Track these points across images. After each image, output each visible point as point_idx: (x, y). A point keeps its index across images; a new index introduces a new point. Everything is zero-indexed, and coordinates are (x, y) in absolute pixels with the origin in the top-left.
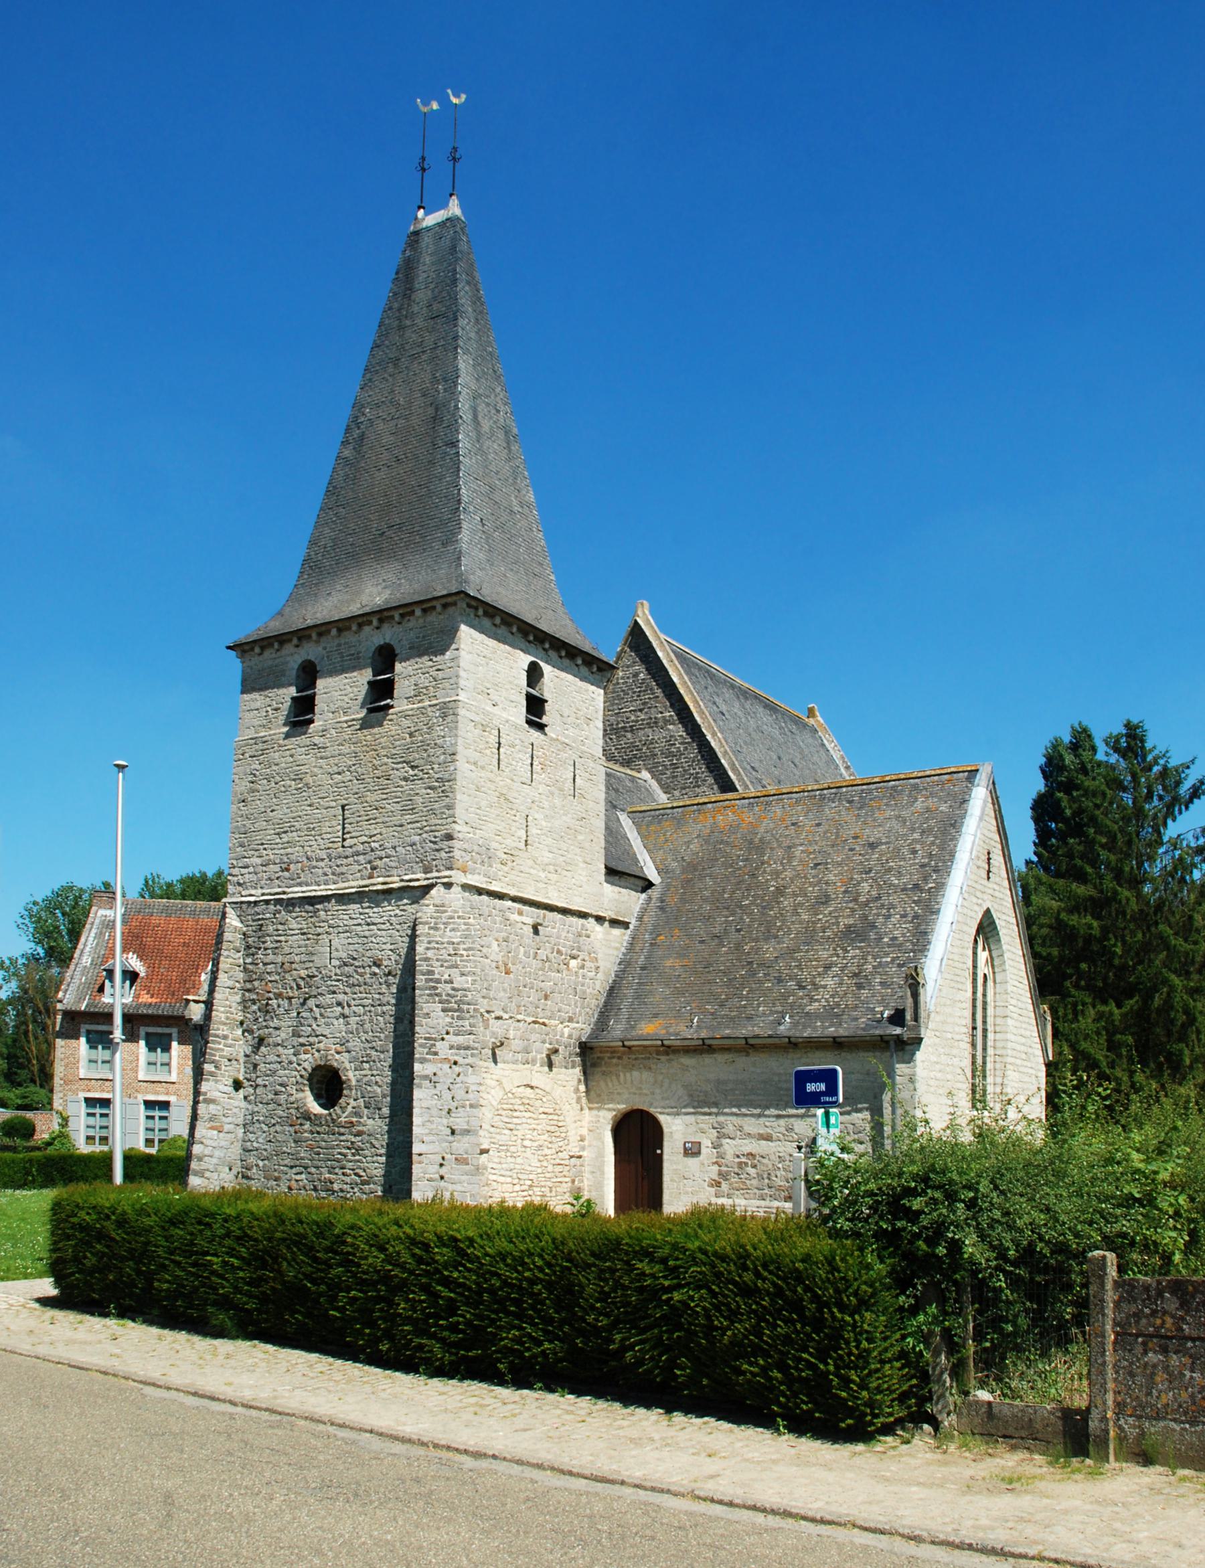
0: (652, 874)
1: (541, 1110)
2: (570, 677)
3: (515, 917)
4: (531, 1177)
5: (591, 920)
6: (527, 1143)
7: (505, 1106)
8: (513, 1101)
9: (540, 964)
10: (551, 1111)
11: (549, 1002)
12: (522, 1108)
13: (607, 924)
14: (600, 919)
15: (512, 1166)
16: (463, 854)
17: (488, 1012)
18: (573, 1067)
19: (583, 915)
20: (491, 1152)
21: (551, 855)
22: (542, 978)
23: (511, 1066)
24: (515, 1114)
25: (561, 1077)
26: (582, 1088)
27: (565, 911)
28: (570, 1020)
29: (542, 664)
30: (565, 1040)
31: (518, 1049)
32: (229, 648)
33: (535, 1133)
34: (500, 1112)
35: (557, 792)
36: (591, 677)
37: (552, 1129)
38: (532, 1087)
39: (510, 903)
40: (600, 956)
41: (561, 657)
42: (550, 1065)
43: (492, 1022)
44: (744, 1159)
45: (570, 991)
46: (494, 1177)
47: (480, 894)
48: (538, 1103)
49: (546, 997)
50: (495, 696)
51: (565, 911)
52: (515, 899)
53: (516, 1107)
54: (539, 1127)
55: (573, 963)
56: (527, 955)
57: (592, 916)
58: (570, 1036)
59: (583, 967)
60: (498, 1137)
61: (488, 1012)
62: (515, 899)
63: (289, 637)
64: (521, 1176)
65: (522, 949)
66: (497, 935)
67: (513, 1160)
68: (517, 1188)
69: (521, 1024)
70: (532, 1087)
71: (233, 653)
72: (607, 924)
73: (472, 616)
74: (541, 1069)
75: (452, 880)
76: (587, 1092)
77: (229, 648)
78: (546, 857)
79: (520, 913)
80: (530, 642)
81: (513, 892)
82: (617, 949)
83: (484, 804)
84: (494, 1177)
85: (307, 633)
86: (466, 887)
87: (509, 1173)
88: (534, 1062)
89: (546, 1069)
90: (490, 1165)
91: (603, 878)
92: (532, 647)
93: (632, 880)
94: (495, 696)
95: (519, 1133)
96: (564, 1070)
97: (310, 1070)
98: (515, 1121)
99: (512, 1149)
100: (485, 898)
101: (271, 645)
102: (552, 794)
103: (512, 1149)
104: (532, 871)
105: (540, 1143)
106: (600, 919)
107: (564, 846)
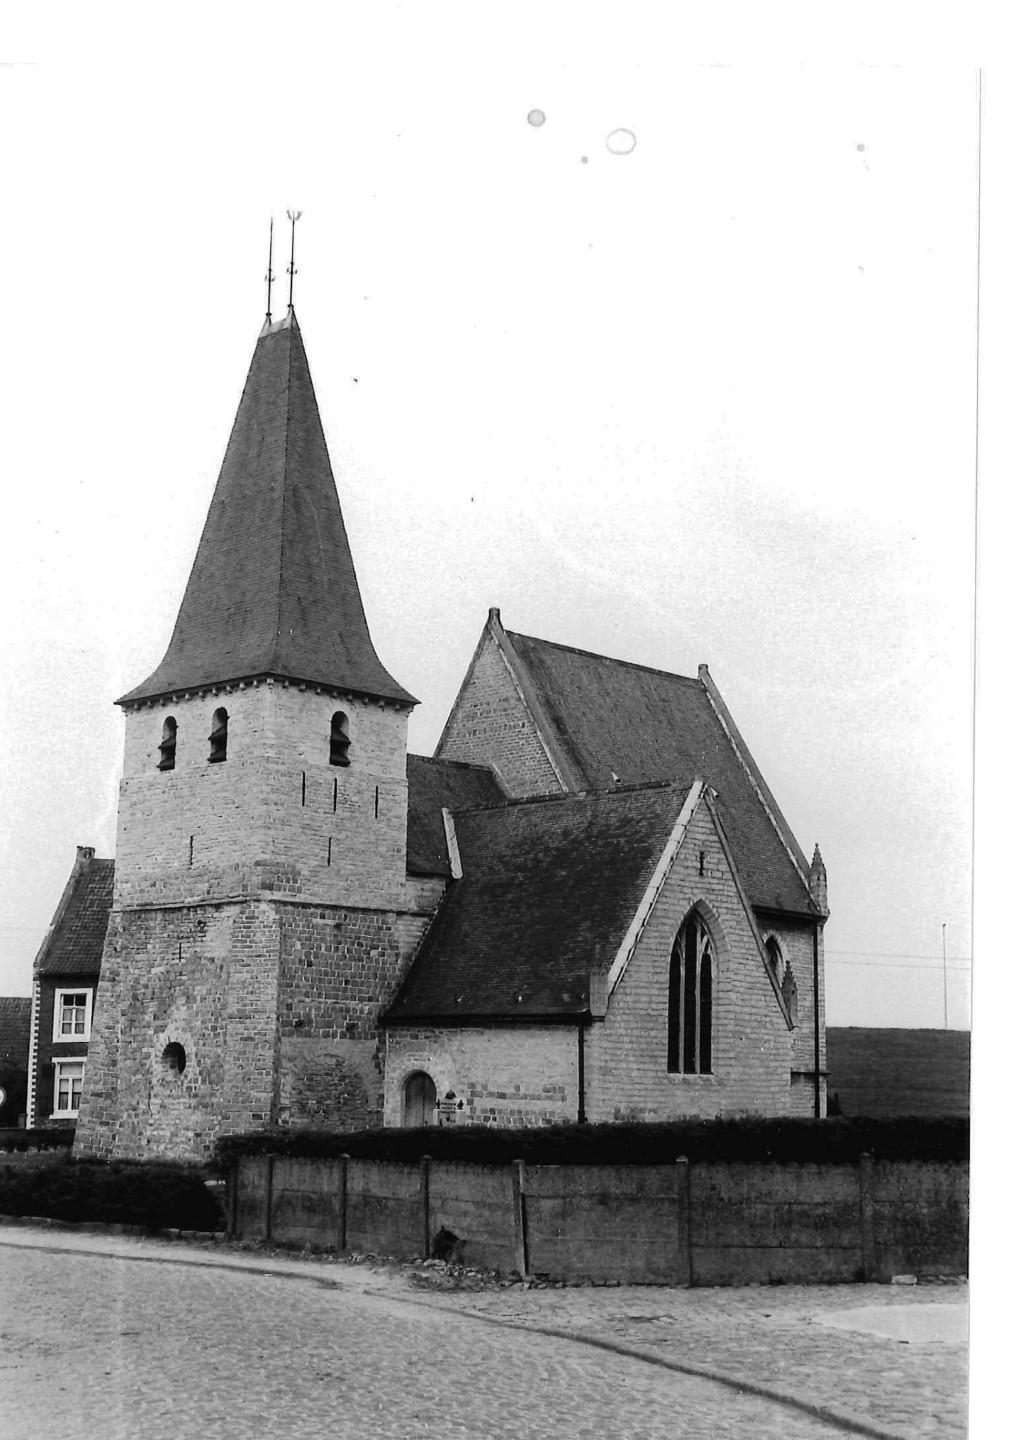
0: (457, 872)
3: (319, 921)
11: (349, 987)
32: (115, 703)
40: (401, 944)
44: (488, 1115)
51: (365, 911)
56: (328, 949)
58: (370, 1013)
59: (383, 955)
63: (157, 698)
65: (323, 946)
71: (119, 707)
75: (260, 897)
77: (115, 703)
79: (323, 917)
85: (169, 696)
88: (334, 1036)
97: (165, 1046)
101: (145, 704)
106: (400, 914)
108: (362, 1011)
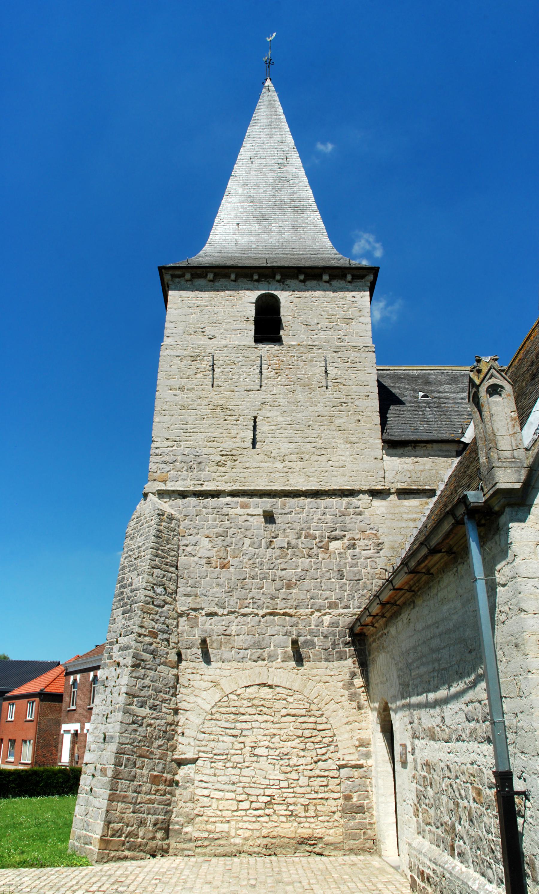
1: (284, 712)
2: (318, 293)
3: (239, 511)
4: (268, 792)
5: (365, 498)
6: (257, 751)
7: (223, 710)
8: (237, 704)
9: (278, 552)
10: (303, 712)
12: (252, 710)
13: (393, 497)
14: (375, 494)
15: (235, 779)
16: (163, 465)
17: (195, 610)
18: (341, 657)
19: (351, 493)
20: (199, 762)
21: (292, 446)
22: (283, 566)
23: (234, 664)
24: (243, 718)
25: (320, 671)
26: (359, 682)
27: (316, 494)
28: (333, 605)
29: (276, 293)
30: (324, 629)
31: (245, 646)
33: (276, 739)
34: (217, 716)
35: (299, 388)
36: (350, 286)
37: (299, 733)
38: (270, 686)
39: (229, 499)
41: (303, 281)
42: (299, 659)
43: (201, 619)
45: (332, 574)
46: (206, 792)
47: (184, 497)
48: (279, 705)
49: (289, 586)
50: (209, 331)
51: (316, 494)
52: (234, 494)
53: (242, 710)
54: (282, 732)
55: (335, 545)
57: (363, 492)
58: (332, 624)
60: (212, 744)
61: (195, 610)
62: (234, 494)
64: (247, 790)
66: (207, 532)
67: (237, 771)
68: (245, 805)
69: (249, 619)
70: (270, 686)
72: (393, 497)
73: (183, 282)
74: (285, 664)
76: (367, 685)
78: (285, 447)
79: (244, 506)
80: (258, 281)
81: (228, 488)
82: (414, 520)
83: (190, 419)
84: (206, 792)
86: (161, 494)
87: (233, 788)
88: (272, 658)
89: (293, 664)
90: (199, 777)
91: (380, 453)
92: (260, 285)
93: (435, 446)
94: (209, 331)
95: (249, 741)
96: (324, 664)
98: (239, 725)
99: (236, 758)
100: (192, 500)
102: (293, 391)
103: (236, 758)
104: (263, 465)
105: (285, 750)
107: (314, 434)
108: (320, 624)
